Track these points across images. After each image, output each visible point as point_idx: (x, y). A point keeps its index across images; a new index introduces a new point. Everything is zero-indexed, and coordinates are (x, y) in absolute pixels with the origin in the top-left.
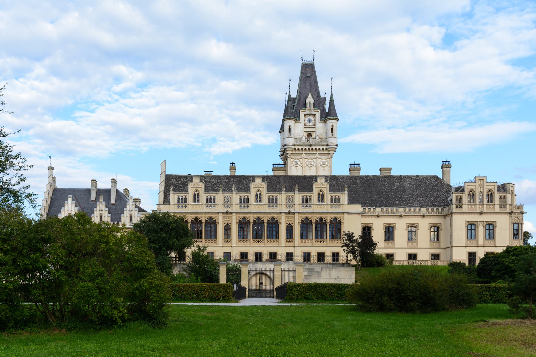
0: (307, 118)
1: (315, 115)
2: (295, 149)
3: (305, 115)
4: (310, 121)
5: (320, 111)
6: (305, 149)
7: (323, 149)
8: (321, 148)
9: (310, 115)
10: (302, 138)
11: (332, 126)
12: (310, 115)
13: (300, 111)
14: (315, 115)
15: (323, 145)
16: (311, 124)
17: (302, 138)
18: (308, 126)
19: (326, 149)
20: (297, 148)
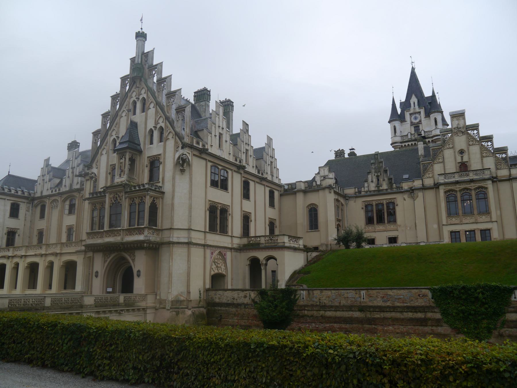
0: (413, 117)
1: (420, 112)
2: (402, 146)
3: (411, 114)
4: (416, 118)
5: (424, 108)
6: (412, 144)
9: (415, 113)
10: (407, 135)
12: (415, 113)
13: (405, 112)
14: (420, 112)
16: (418, 121)
17: (407, 135)
18: (415, 123)
19: (432, 141)
20: (403, 145)
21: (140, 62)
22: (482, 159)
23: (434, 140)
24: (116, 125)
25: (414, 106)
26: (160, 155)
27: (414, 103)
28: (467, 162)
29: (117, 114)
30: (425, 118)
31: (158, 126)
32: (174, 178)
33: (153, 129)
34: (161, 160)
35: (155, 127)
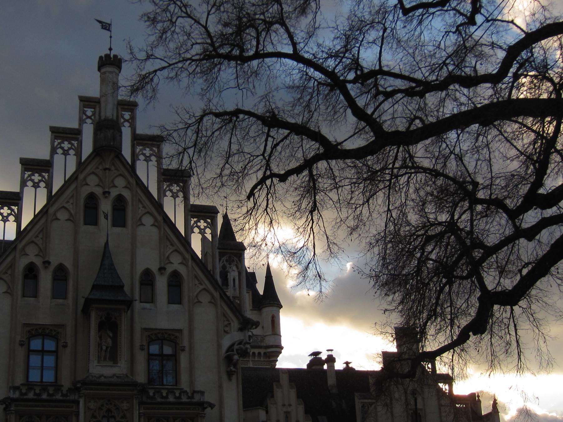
7: (259, 353)
8: (256, 351)
11: (273, 317)
15: (260, 347)
19: (265, 353)
21: (115, 118)
22: (440, 409)
23: (268, 352)
24: (39, 233)
25: (234, 285)
26: (180, 331)
27: (234, 280)
28: (421, 409)
29: (45, 210)
30: (251, 310)
31: (170, 269)
32: (220, 387)
33: (154, 268)
34: (186, 343)
35: (162, 269)
